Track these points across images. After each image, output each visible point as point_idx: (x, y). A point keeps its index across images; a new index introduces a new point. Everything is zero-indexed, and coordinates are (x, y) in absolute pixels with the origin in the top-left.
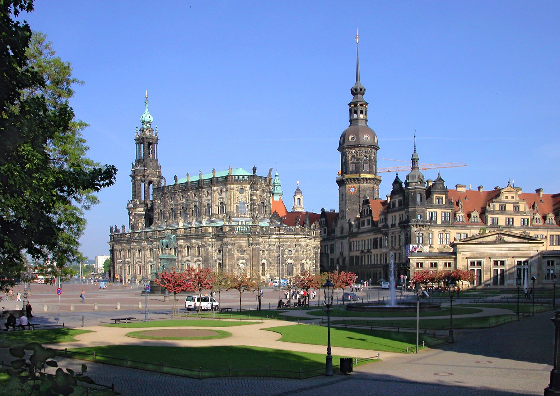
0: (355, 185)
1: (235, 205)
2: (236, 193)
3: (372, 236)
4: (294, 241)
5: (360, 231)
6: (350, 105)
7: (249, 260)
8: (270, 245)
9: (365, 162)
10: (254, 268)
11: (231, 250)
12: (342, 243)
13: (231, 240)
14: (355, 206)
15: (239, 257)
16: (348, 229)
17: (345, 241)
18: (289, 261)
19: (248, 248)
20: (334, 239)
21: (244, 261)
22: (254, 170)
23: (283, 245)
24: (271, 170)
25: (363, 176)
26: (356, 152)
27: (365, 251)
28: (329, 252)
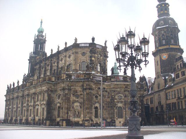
1: (78, 65)
5: (175, 82)
7: (82, 104)
9: (172, 38)
10: (87, 111)
12: (159, 95)
15: (74, 100)
17: (162, 94)
18: (120, 105)
19: (82, 93)
21: (78, 104)
22: (93, 39)
23: (114, 91)
24: (106, 42)
25: (171, 46)
26: (165, 32)
27: (182, 97)
28: (149, 103)
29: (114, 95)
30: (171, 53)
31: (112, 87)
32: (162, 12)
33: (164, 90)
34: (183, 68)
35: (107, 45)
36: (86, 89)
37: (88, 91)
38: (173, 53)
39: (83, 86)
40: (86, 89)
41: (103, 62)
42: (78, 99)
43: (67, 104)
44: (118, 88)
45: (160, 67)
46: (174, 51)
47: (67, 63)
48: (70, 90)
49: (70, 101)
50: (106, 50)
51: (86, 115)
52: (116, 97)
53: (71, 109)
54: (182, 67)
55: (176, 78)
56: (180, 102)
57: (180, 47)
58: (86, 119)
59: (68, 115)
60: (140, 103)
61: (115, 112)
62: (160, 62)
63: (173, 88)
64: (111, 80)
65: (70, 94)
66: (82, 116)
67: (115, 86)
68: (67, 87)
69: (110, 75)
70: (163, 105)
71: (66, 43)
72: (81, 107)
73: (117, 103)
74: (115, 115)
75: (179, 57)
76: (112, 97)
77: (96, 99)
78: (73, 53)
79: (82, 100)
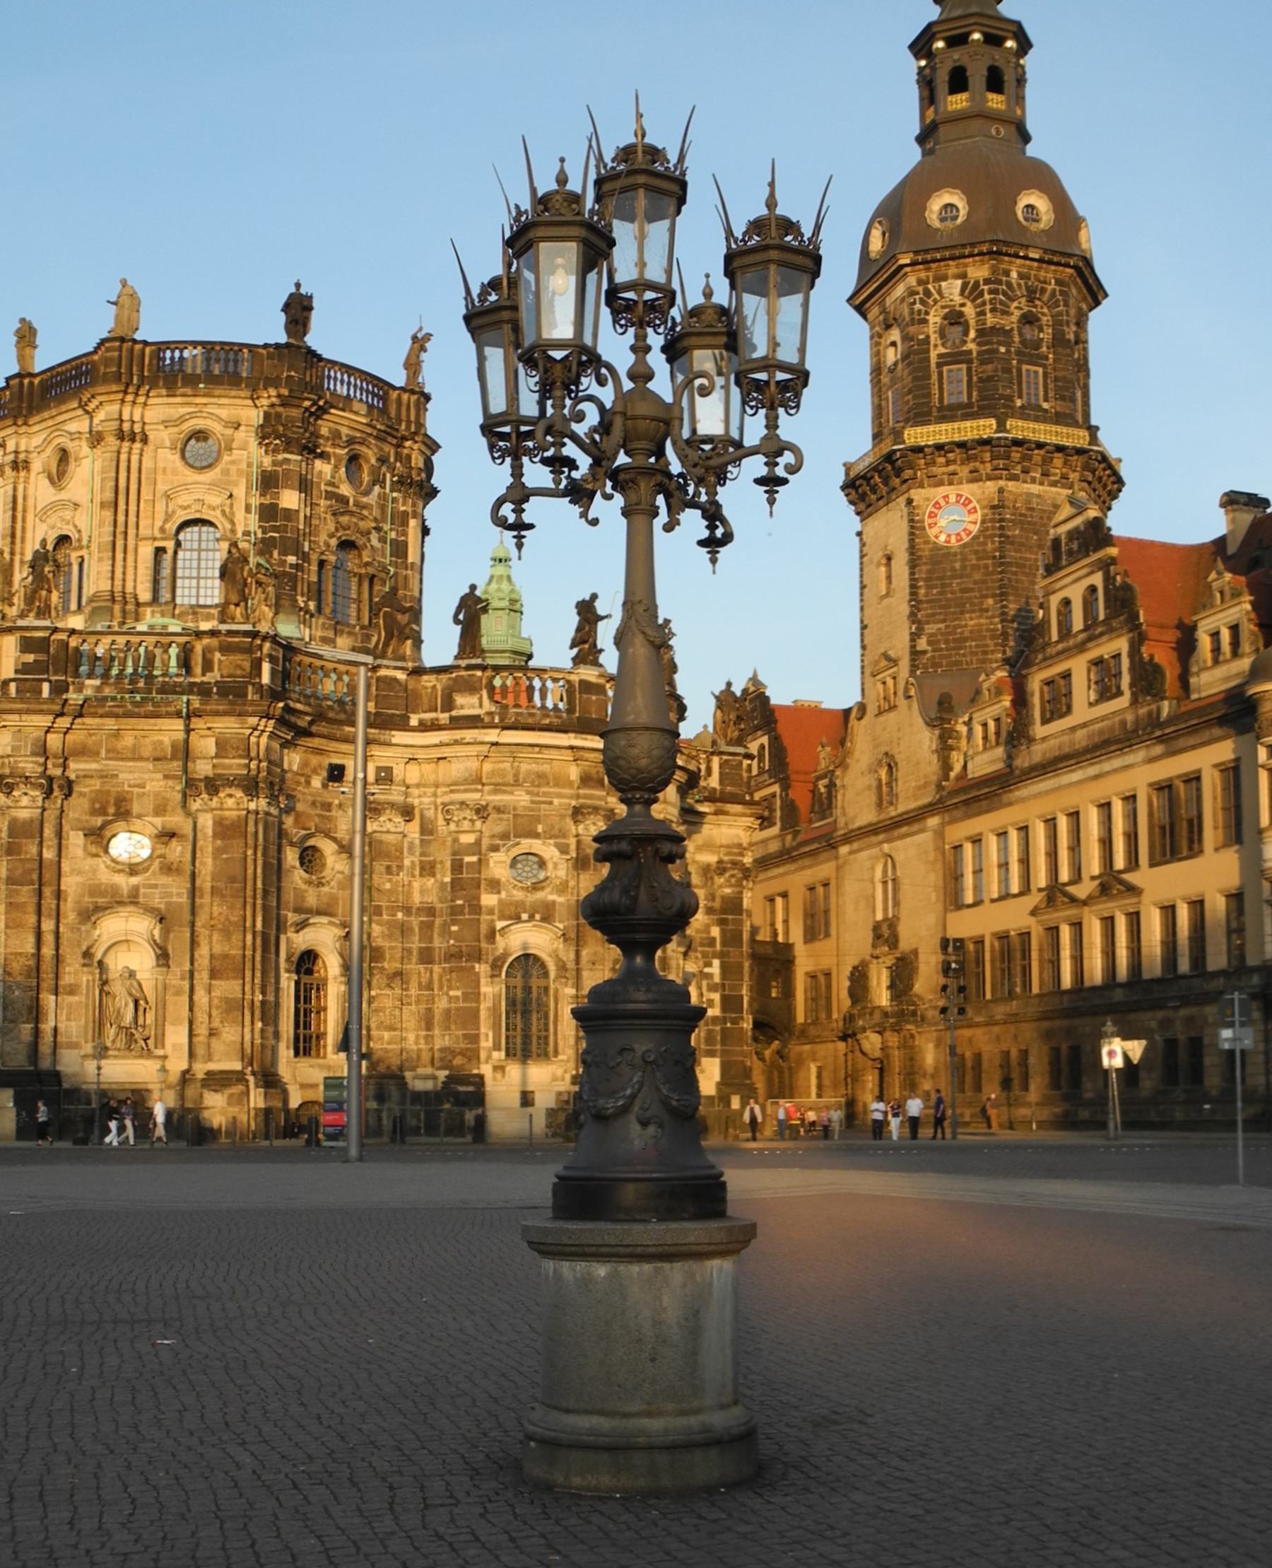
0: (968, 490)
2: (161, 457)
3: (1141, 772)
4: (561, 781)
6: (921, 46)
8: (372, 809)
9: (1030, 352)
11: (34, 830)
13: (42, 750)
14: (972, 622)
15: (95, 890)
16: (931, 765)
20: (829, 843)
23: (481, 812)
25: (1019, 428)
26: (972, 291)
29: (478, 843)
30: (1011, 486)
31: (457, 769)
32: (958, 102)
33: (933, 822)
34: (1111, 630)
35: (430, 379)
36: (212, 785)
37: (230, 802)
38: (1035, 489)
39: (184, 752)
40: (212, 785)
41: (382, 540)
42: (134, 880)
43: (32, 919)
44: (517, 783)
45: (905, 609)
46: (1045, 474)
47: (38, 534)
48: (57, 787)
49: (59, 894)
50: (420, 425)
51: (212, 1033)
52: (498, 865)
53: (66, 980)
54: (1096, 623)
55: (1045, 721)
56: (1066, 933)
57: (1094, 439)
58: (213, 1066)
59: (37, 1032)
60: (715, 932)
61: (484, 1007)
62: (913, 564)
63: (1010, 804)
64: (448, 705)
65: (59, 834)
66: (177, 1036)
67: (487, 767)
68: (30, 766)
69: (448, 660)
70: (915, 952)
71: (26, 336)
72: (163, 957)
73: (500, 925)
74: (484, 1029)
75: (1076, 529)
76: (457, 866)
77: (310, 883)
78: (96, 439)
79: (177, 890)
